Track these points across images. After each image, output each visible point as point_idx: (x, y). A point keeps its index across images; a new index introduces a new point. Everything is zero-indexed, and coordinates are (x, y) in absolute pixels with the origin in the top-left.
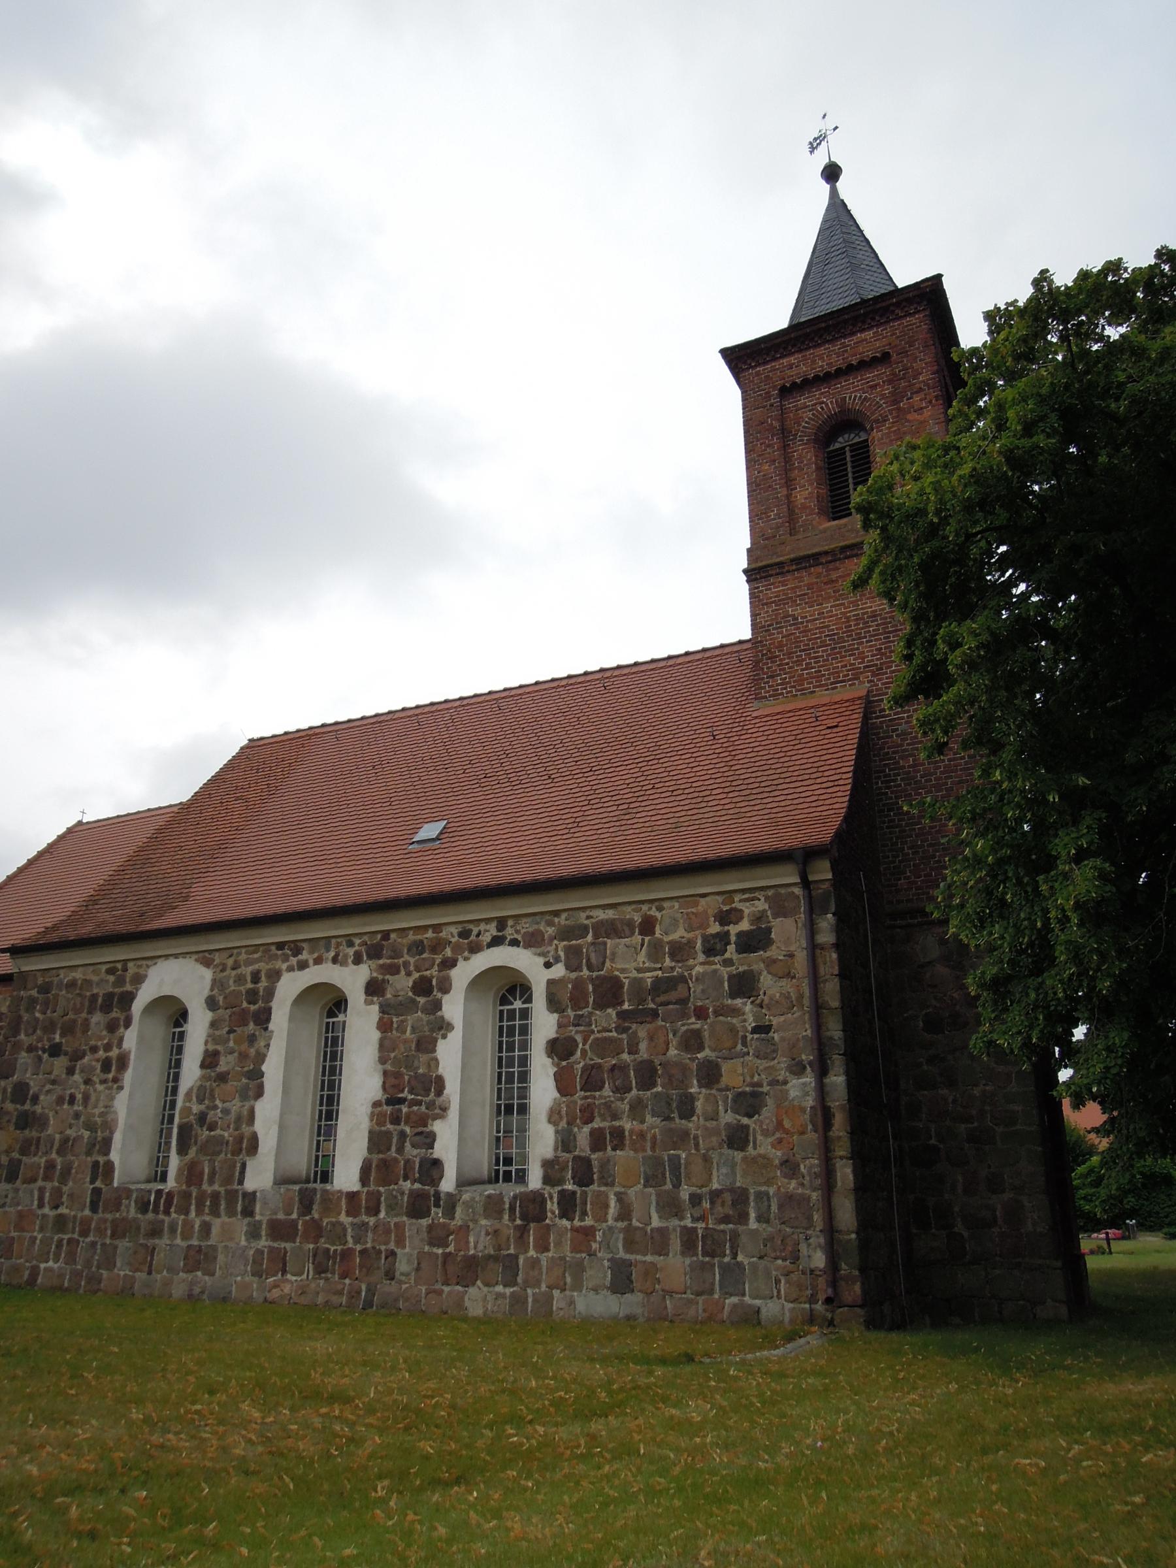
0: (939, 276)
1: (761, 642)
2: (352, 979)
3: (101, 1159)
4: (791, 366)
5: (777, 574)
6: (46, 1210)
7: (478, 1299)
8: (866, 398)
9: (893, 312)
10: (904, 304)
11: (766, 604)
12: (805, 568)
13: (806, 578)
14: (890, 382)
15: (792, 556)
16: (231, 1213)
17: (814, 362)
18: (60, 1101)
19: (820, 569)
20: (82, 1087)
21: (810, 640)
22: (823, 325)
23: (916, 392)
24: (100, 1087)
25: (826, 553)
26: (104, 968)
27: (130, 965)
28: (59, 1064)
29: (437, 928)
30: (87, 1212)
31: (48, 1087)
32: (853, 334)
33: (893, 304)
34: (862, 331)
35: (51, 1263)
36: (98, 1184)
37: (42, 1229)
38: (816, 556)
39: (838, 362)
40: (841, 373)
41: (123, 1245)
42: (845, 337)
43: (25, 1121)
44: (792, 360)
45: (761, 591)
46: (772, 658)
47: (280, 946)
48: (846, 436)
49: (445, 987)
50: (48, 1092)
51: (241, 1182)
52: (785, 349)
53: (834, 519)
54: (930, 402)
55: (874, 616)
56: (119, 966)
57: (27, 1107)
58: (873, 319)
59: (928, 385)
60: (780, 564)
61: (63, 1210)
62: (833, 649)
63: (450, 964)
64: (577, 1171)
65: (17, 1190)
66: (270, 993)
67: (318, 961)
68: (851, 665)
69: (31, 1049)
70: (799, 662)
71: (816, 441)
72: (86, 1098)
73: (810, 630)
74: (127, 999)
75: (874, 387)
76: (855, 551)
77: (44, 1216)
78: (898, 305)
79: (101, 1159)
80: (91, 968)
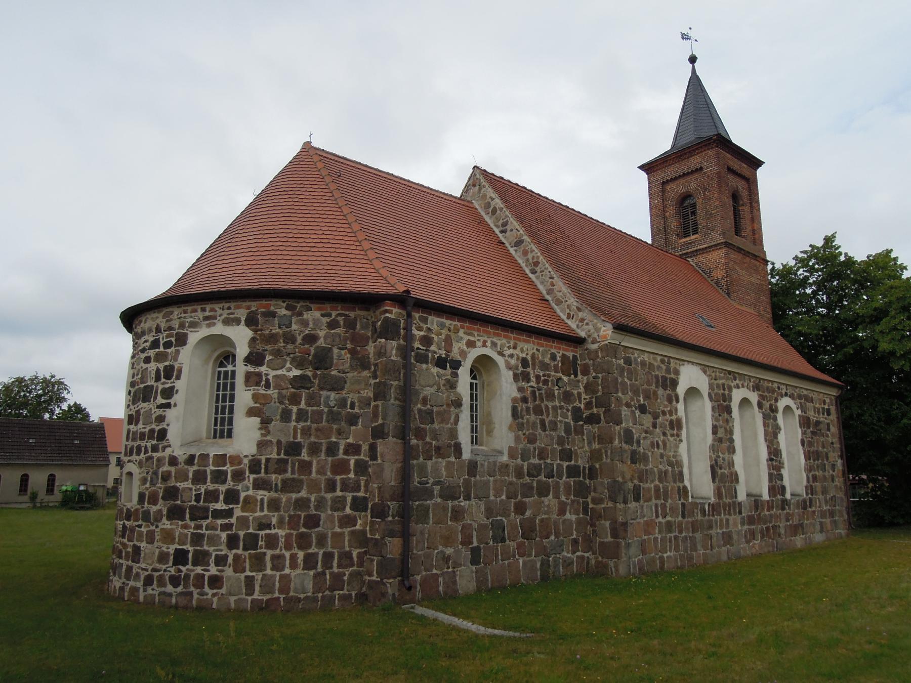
2: (754, 397)
3: (681, 485)
6: (660, 519)
7: (799, 541)
16: (735, 514)
18: (652, 445)
20: (662, 437)
24: (671, 439)
26: (659, 358)
27: (672, 361)
28: (647, 420)
29: (773, 382)
30: (680, 518)
31: (644, 435)
35: (669, 553)
36: (682, 500)
37: (660, 532)
41: (698, 536)
43: (635, 458)
47: (730, 373)
49: (776, 411)
50: (645, 438)
51: (736, 497)
56: (666, 359)
57: (635, 447)
61: (669, 518)
63: (776, 400)
64: (810, 489)
65: (642, 507)
66: (730, 399)
67: (743, 386)
69: (628, 405)
72: (665, 445)
74: (674, 383)
77: (660, 523)
79: (681, 485)
80: (652, 356)
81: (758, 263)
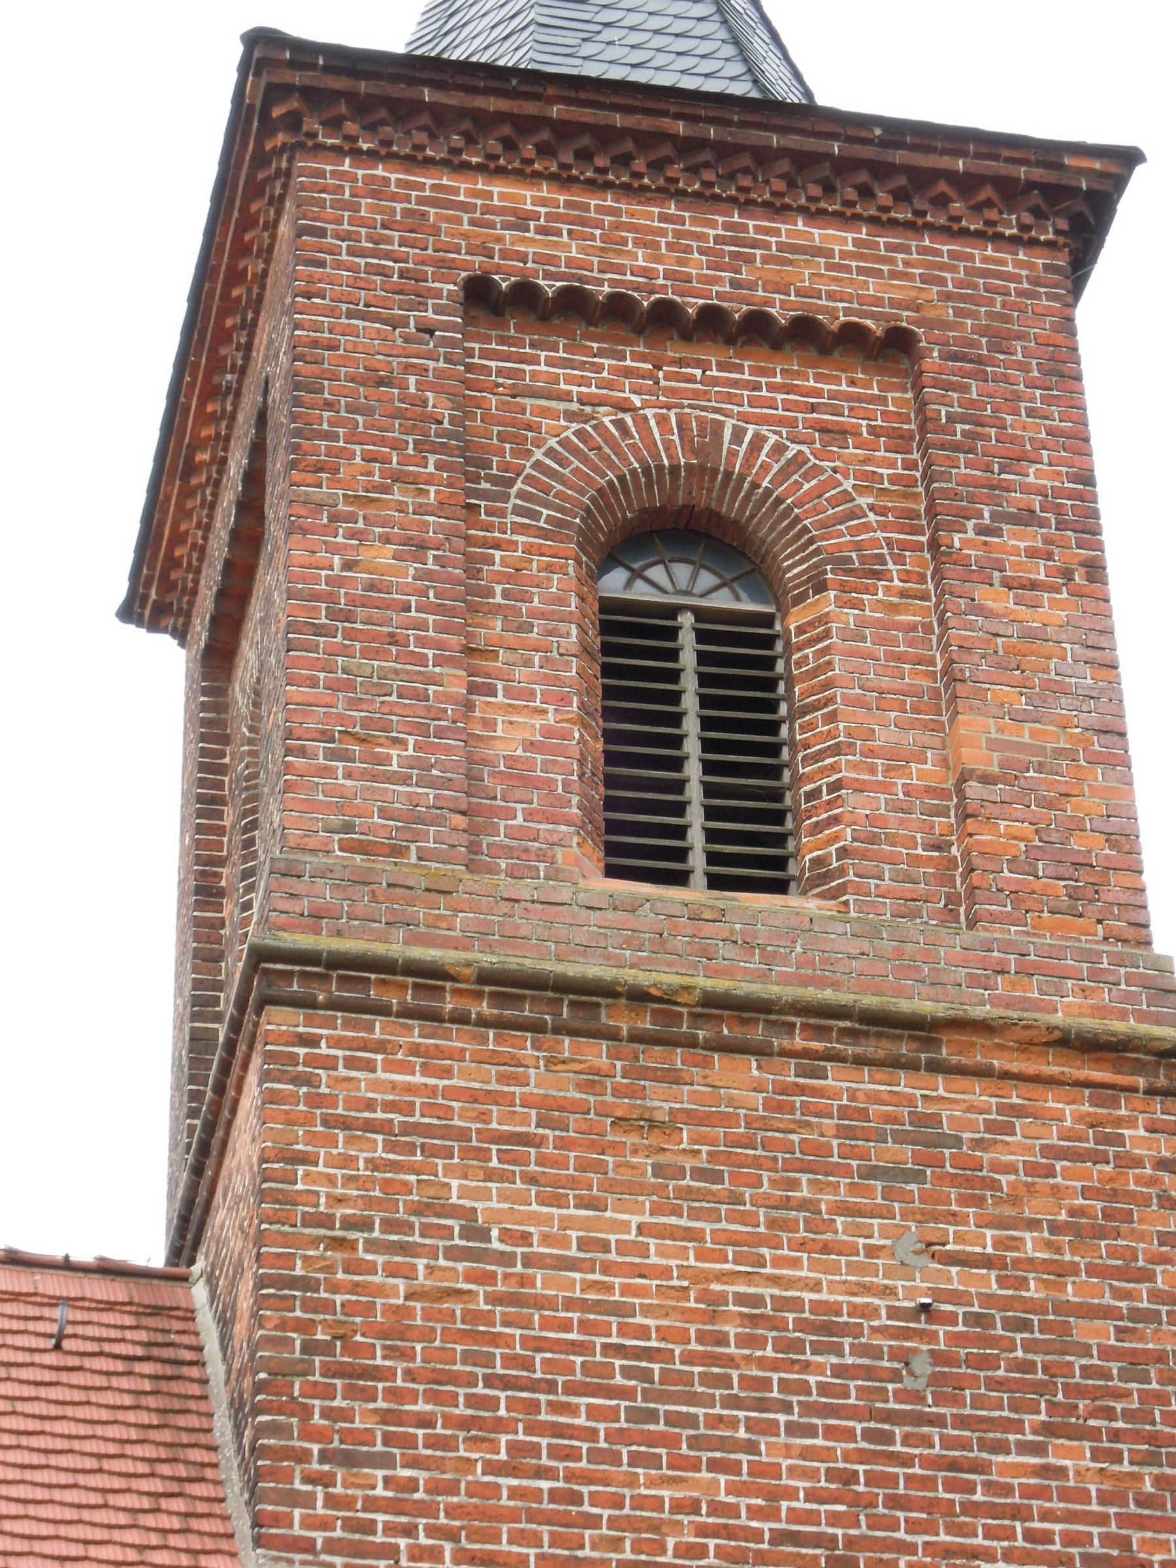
0: (1129, 158)
1: (306, 1284)
4: (521, 220)
5: (335, 1005)
8: (798, 461)
9: (942, 202)
10: (987, 192)
11: (345, 1124)
12: (536, 1028)
13: (547, 1070)
14: (899, 441)
15: (488, 960)
17: (612, 242)
19: (598, 1054)
21: (539, 1345)
22: (681, 128)
23: (1014, 520)
25: (639, 997)
32: (778, 209)
33: (951, 176)
34: (815, 215)
38: (588, 995)
39: (704, 285)
40: (757, 332)
42: (746, 206)
44: (527, 196)
45: (329, 1064)
46: (358, 1377)
48: (682, 571)
52: (509, 145)
53: (612, 872)
54: (1068, 575)
55: (827, 1327)
58: (866, 192)
59: (1058, 510)
60: (430, 975)
62: (635, 1415)
68: (717, 1508)
70: (482, 1428)
71: (586, 540)
73: (540, 1303)
75: (836, 434)
76: (758, 1033)
78: (966, 184)
81: (962, 1106)
